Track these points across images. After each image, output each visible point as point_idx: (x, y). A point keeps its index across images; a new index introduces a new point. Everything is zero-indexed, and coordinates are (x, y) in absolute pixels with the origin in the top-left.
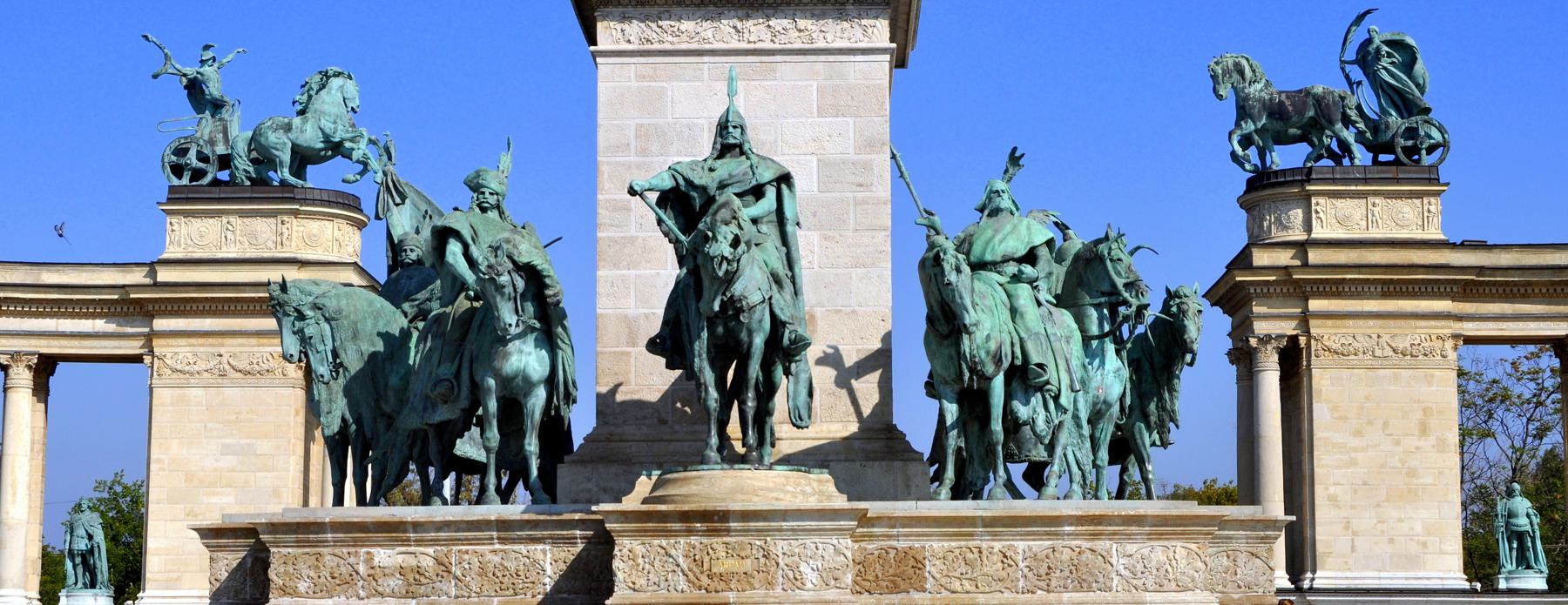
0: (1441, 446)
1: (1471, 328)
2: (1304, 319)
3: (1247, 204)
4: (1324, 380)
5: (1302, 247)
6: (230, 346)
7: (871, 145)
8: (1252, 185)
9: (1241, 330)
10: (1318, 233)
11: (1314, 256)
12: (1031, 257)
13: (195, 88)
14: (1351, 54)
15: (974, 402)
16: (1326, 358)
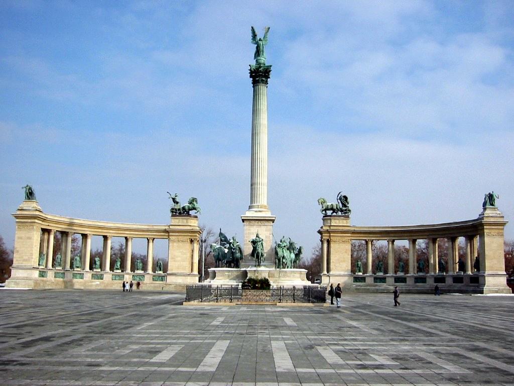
0: (348, 255)
1: (353, 238)
2: (330, 236)
3: (323, 220)
4: (332, 245)
5: (330, 226)
6: (180, 237)
7: (270, 234)
8: (324, 217)
9: (322, 238)
10: (332, 224)
11: (331, 228)
12: (285, 247)
13: (174, 199)
14: (338, 198)
15: (279, 260)
16: (333, 242)
